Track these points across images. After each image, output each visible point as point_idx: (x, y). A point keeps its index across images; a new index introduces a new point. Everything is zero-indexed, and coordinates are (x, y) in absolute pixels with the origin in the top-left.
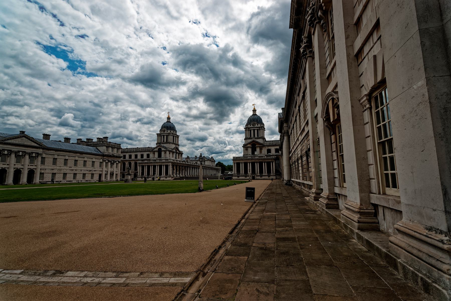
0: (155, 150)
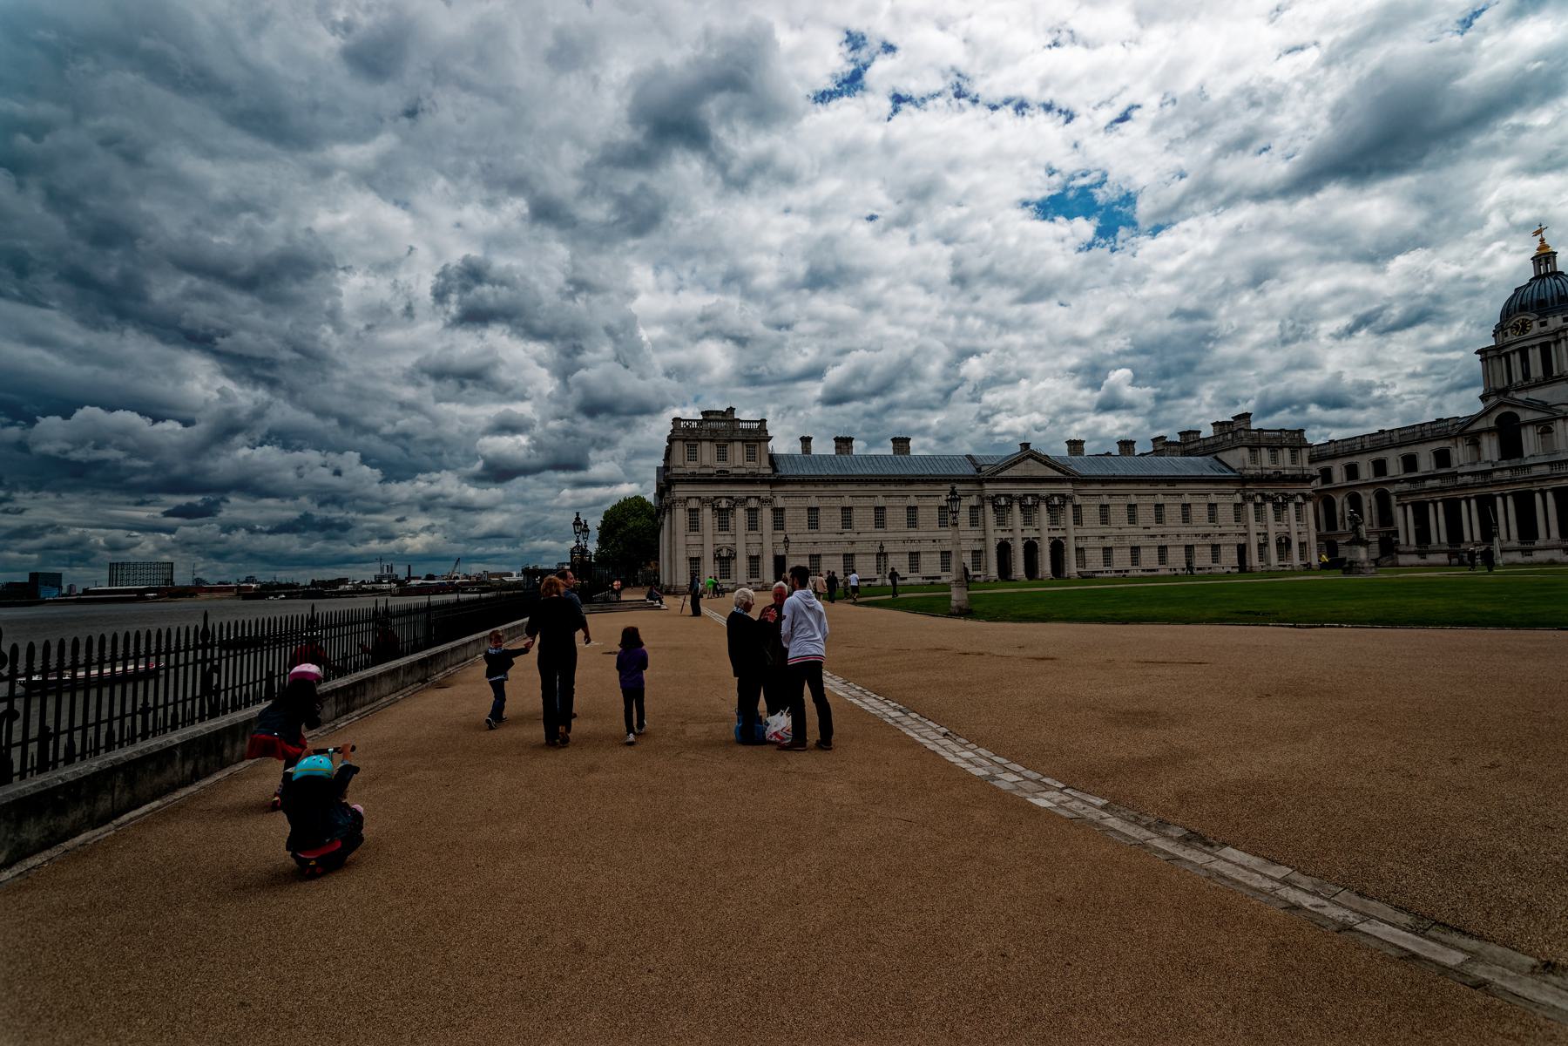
0: (1476, 427)
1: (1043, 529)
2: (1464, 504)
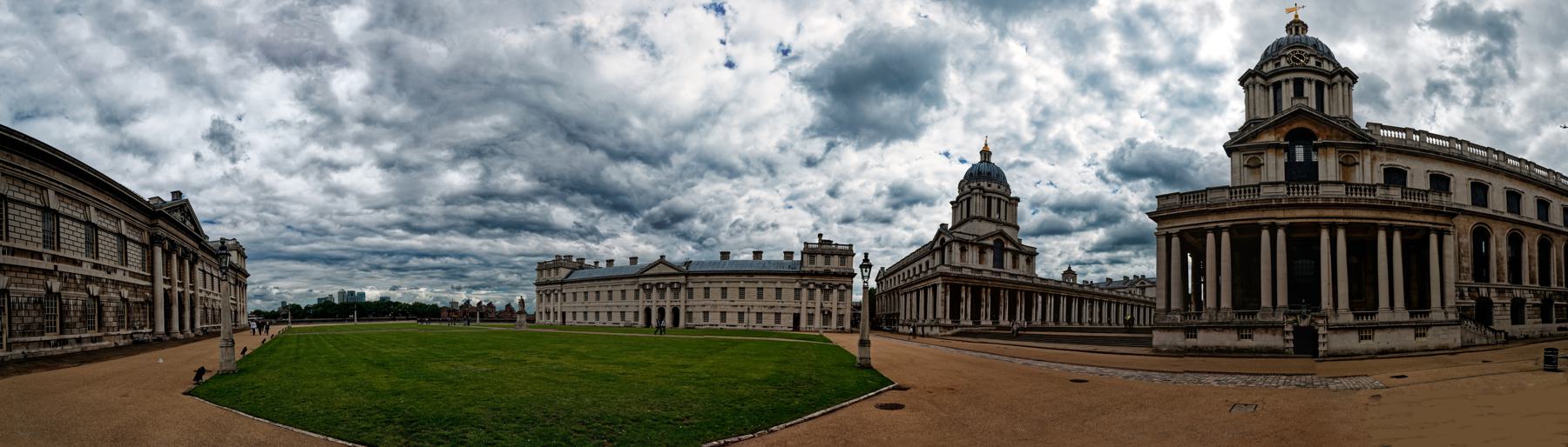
1: (668, 301)
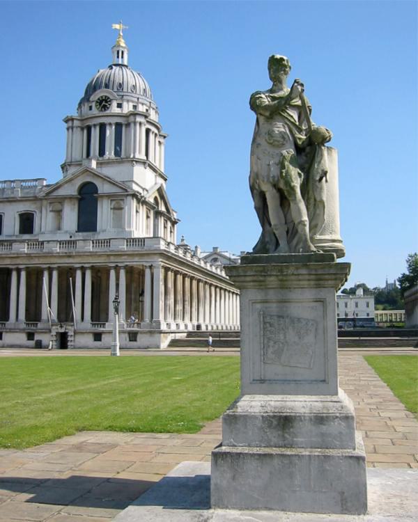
2: (79, 274)
